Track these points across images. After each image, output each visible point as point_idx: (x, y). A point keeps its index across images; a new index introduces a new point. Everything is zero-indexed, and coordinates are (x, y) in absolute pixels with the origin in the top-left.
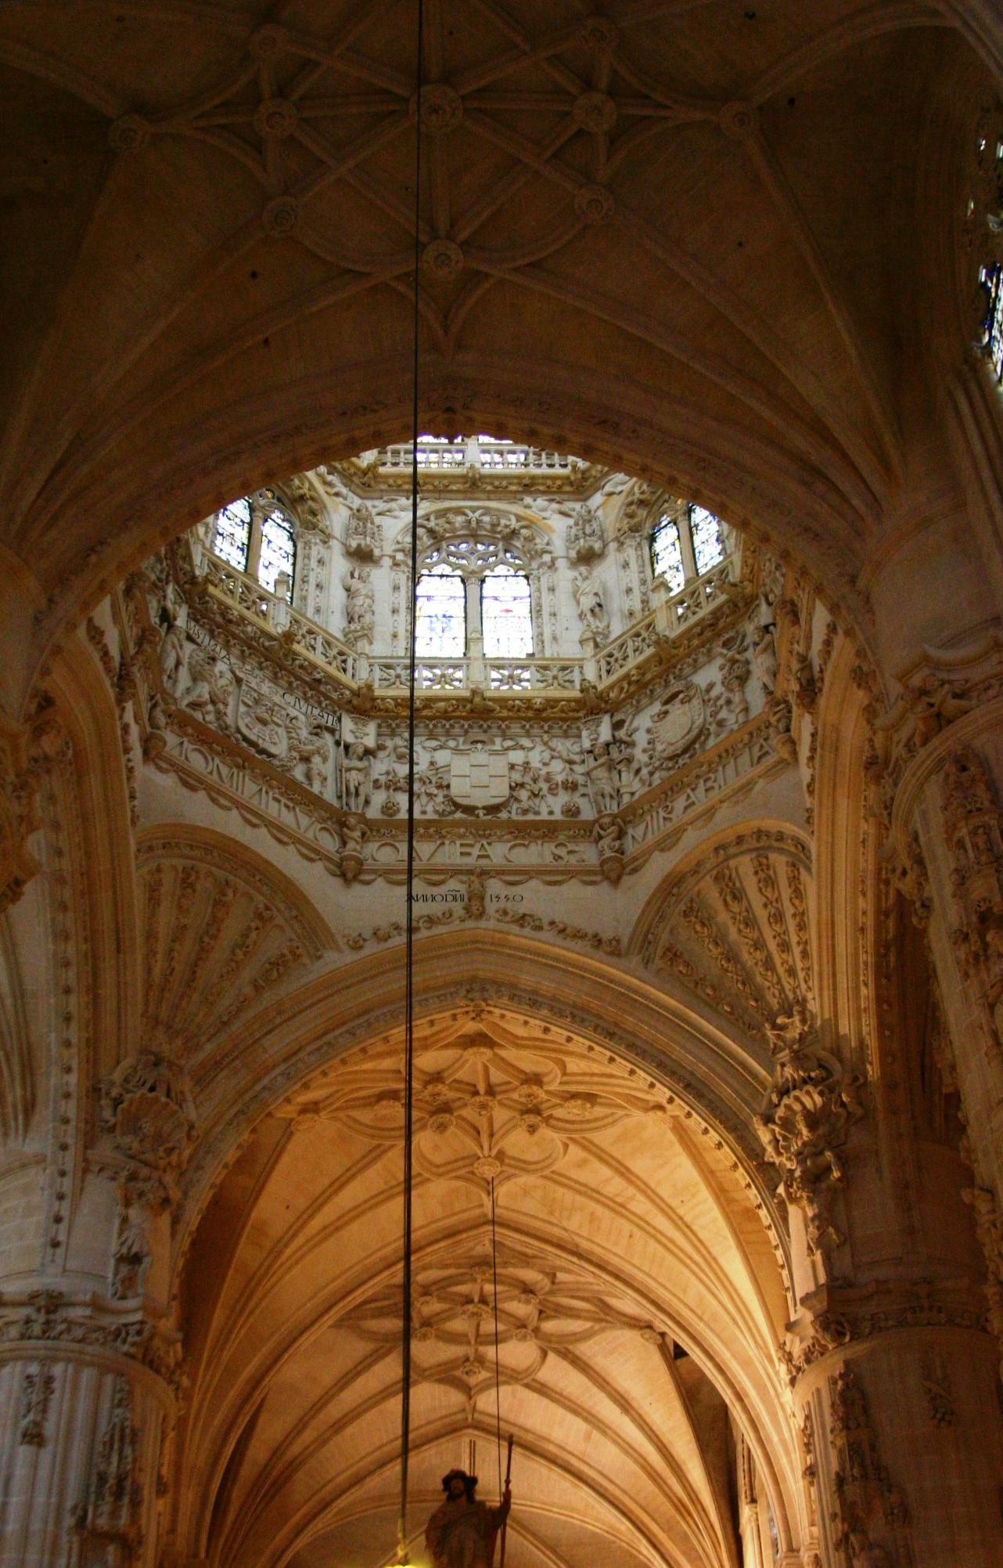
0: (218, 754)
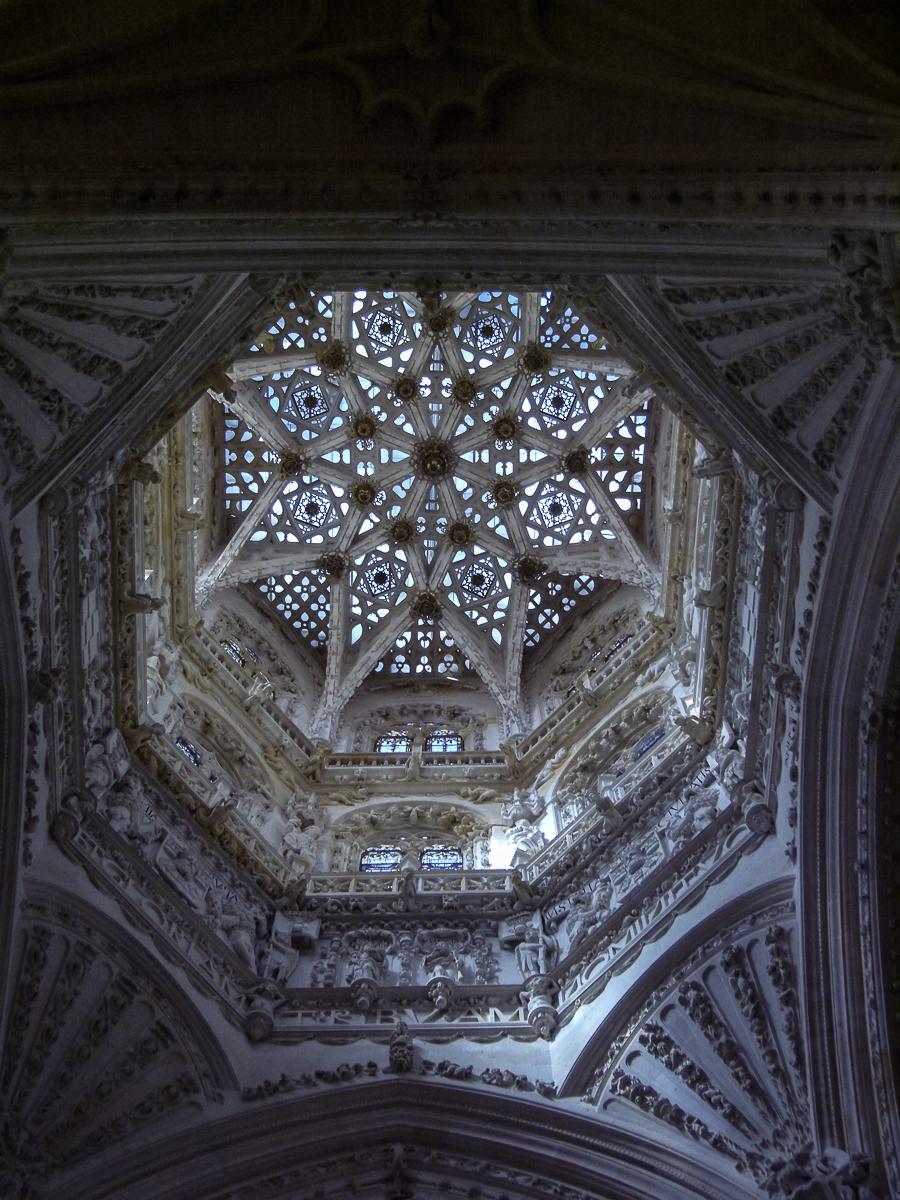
0: (610, 942)
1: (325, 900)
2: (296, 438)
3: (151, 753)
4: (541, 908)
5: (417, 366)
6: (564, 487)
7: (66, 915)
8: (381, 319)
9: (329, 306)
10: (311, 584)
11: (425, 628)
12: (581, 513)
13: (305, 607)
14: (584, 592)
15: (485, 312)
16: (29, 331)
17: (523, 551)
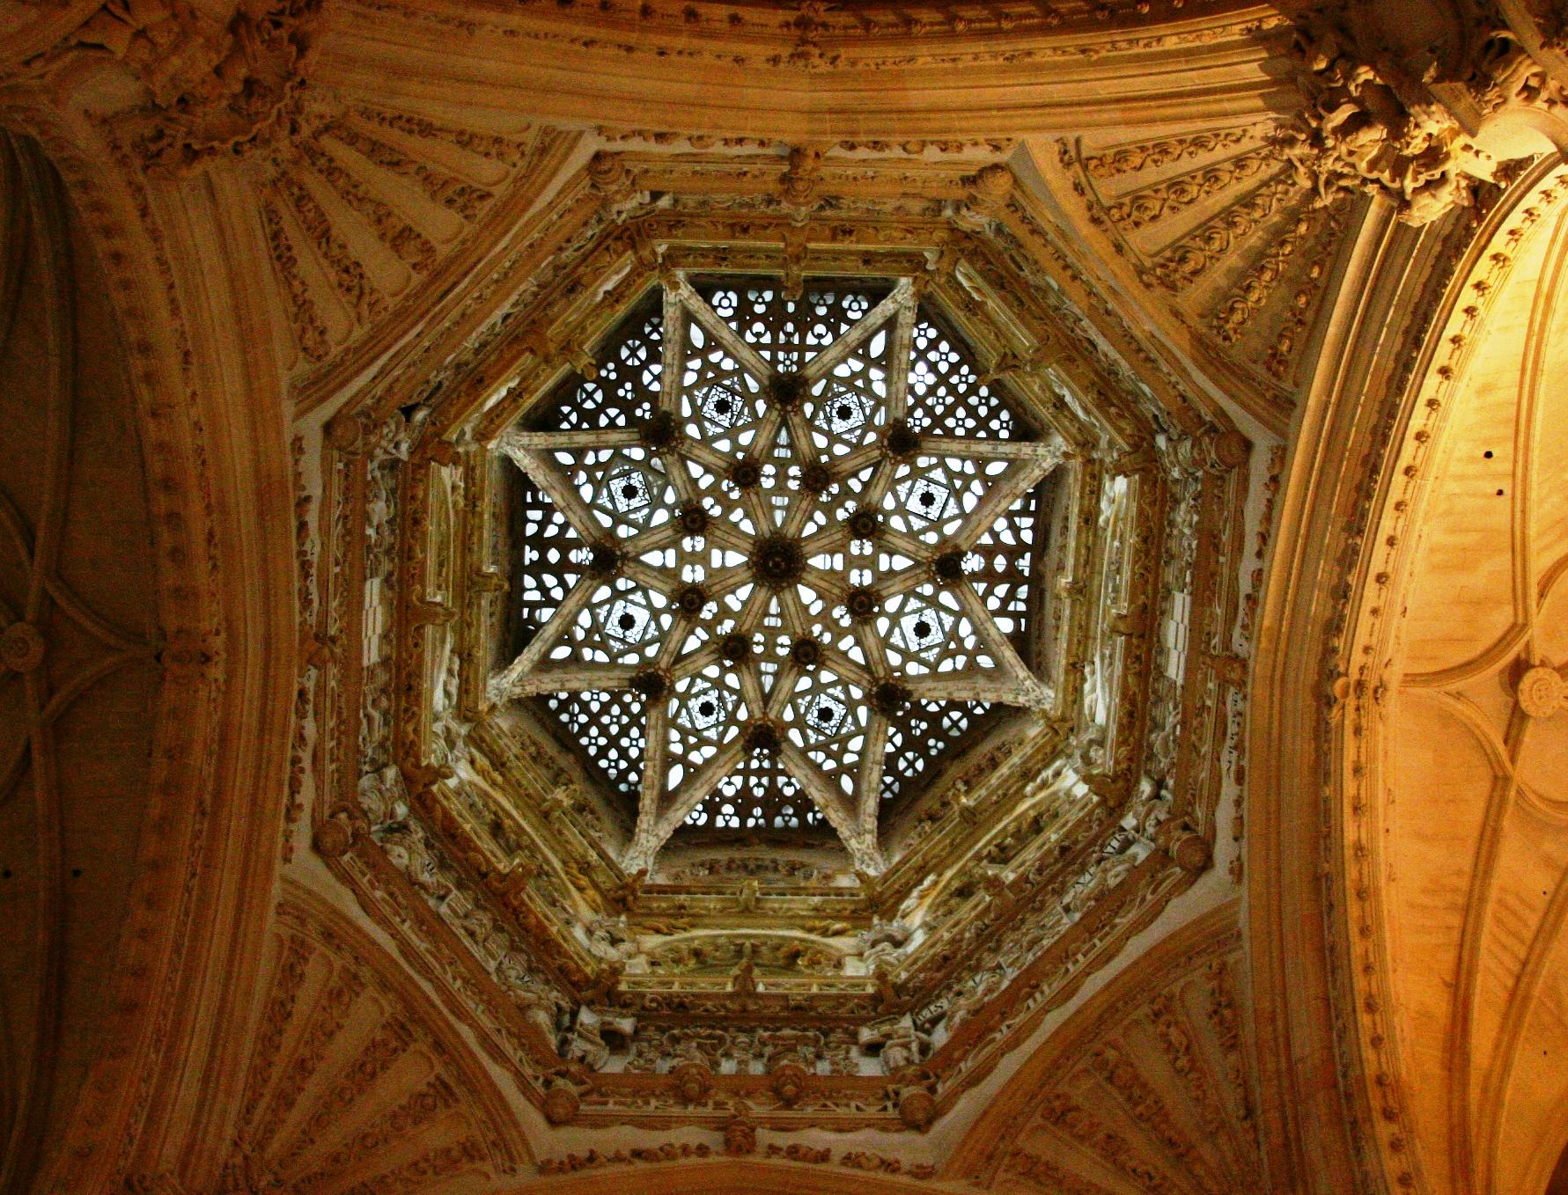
1: (643, 996)
2: (610, 531)
3: (435, 800)
4: (911, 1010)
5: (759, 447)
6: (933, 602)
7: (330, 935)
8: (717, 394)
9: (657, 378)
10: (622, 713)
11: (760, 772)
12: (953, 635)
13: (614, 742)
14: (955, 733)
15: (842, 389)
16: (331, 171)
17: (882, 673)
